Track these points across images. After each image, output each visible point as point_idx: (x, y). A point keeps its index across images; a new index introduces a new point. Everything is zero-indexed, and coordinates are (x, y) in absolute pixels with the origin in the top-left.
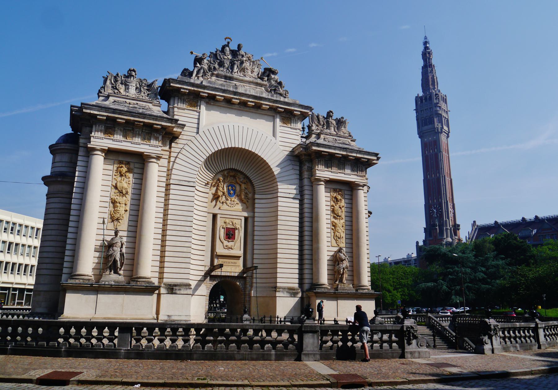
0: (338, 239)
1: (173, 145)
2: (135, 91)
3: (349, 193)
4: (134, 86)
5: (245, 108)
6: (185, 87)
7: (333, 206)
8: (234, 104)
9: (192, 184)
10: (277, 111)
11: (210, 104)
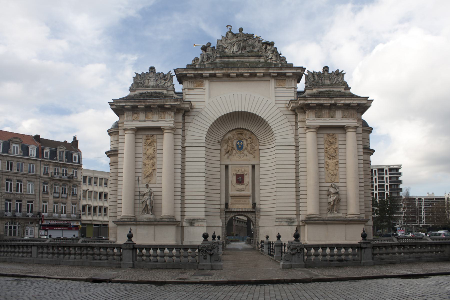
0: (332, 176)
1: (186, 117)
2: (155, 83)
3: (343, 135)
4: (154, 79)
5: (243, 78)
7: (327, 148)
8: (232, 77)
9: (202, 145)
10: (272, 76)
11: (214, 81)
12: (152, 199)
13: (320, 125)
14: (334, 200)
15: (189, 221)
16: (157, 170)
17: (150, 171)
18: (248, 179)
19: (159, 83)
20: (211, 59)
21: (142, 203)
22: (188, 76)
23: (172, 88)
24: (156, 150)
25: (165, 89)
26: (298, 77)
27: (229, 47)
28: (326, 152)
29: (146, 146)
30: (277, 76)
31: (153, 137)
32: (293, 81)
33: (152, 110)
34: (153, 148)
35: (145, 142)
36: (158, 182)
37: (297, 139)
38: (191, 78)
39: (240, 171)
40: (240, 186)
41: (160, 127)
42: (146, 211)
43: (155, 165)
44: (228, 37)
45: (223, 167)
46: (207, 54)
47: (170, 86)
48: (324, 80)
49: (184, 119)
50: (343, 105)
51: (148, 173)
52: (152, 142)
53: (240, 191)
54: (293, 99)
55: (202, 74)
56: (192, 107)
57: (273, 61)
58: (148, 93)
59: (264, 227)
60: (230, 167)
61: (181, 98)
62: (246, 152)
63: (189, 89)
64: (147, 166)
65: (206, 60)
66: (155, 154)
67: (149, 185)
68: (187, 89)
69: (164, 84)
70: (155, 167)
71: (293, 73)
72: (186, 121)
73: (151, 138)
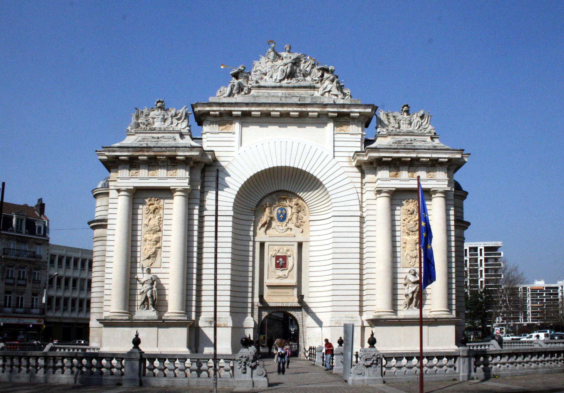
1: (206, 174)
6: (215, 108)
7: (404, 220)
12: (155, 289)
13: (395, 188)
14: (413, 293)
15: (207, 320)
16: (162, 248)
17: (153, 250)
18: (292, 262)
19: (169, 124)
20: (244, 90)
21: (140, 294)
22: (212, 114)
23: (188, 131)
24: (163, 221)
25: (177, 133)
26: (367, 120)
27: (270, 72)
28: (403, 225)
29: (148, 215)
30: (338, 116)
31: (157, 202)
32: (360, 124)
33: (158, 163)
34: (158, 217)
35: (147, 208)
36: (163, 265)
37: (361, 207)
38: (215, 116)
39: (281, 251)
40: (280, 273)
41: (169, 187)
42: (146, 306)
43: (161, 242)
44: (269, 58)
45: (258, 245)
46: (240, 84)
47: (185, 128)
48: (403, 124)
49: (203, 177)
50: (428, 160)
51: (150, 253)
52: (157, 208)
53: (281, 278)
54: (359, 150)
55: (231, 111)
56: (215, 160)
57: (332, 94)
58: (153, 138)
59: (313, 328)
60: (266, 245)
61: (199, 145)
62: (290, 225)
63: (211, 133)
64: (148, 242)
65: (237, 91)
66: (161, 225)
67: (151, 269)
68: (209, 132)
69: (175, 125)
70: (161, 244)
71: (360, 113)
72: (206, 179)
73: (156, 202)
